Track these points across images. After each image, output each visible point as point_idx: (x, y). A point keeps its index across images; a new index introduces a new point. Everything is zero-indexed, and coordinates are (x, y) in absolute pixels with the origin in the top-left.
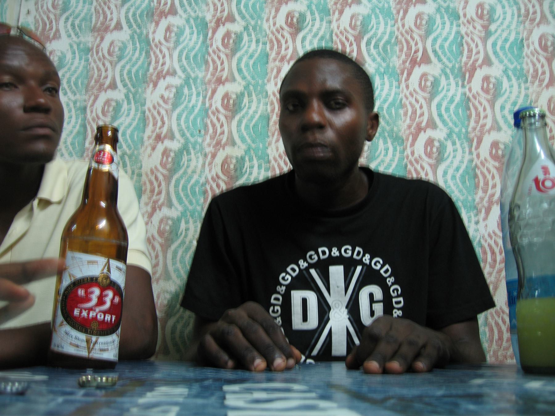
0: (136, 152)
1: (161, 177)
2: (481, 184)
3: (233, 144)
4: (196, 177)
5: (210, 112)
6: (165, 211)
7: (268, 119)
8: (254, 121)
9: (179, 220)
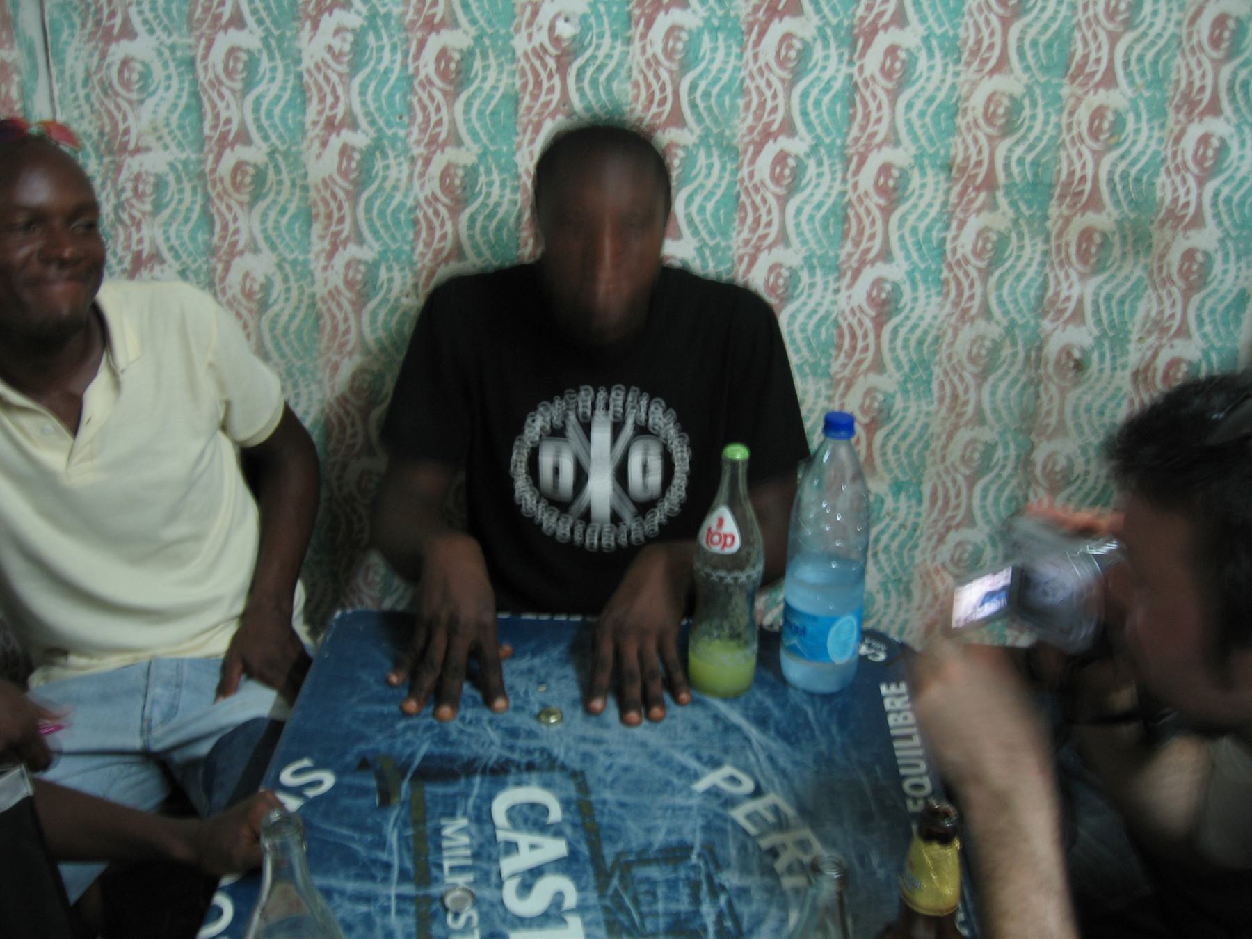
0: (294, 149)
1: (341, 195)
2: (853, 232)
3: (459, 143)
4: (398, 197)
5: (416, 83)
6: (352, 251)
7: (517, 101)
8: (493, 103)
9: (375, 265)
